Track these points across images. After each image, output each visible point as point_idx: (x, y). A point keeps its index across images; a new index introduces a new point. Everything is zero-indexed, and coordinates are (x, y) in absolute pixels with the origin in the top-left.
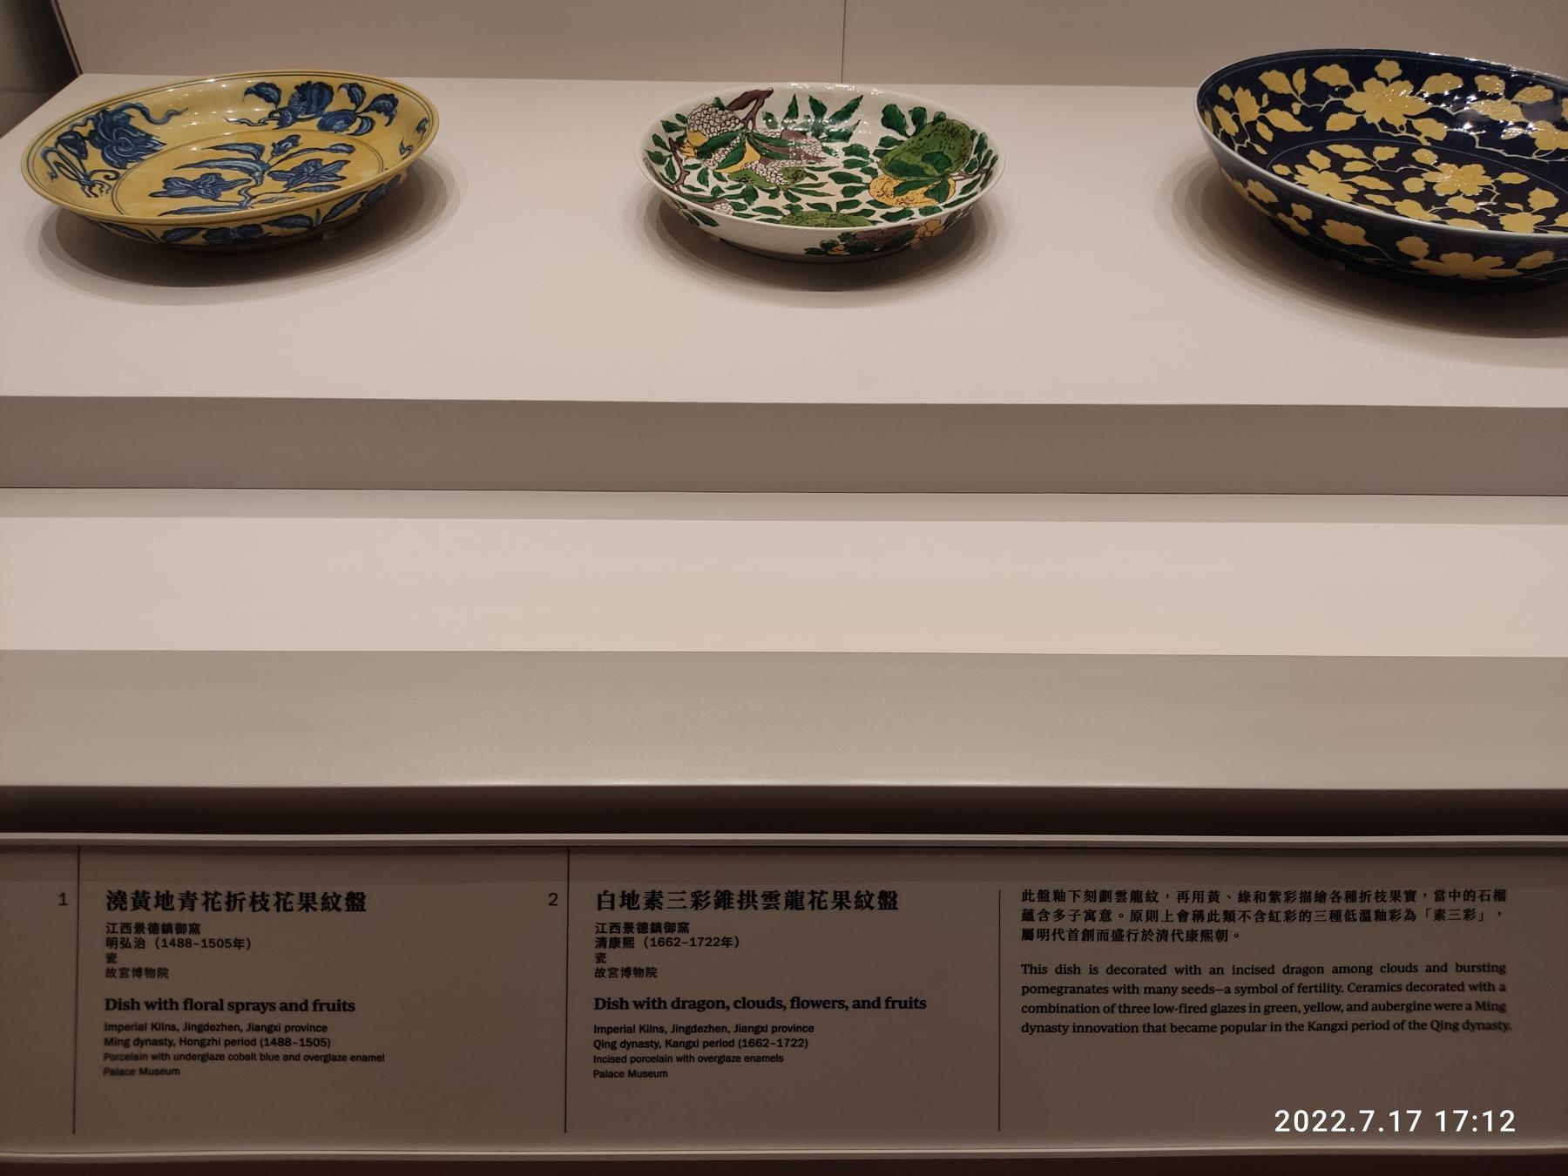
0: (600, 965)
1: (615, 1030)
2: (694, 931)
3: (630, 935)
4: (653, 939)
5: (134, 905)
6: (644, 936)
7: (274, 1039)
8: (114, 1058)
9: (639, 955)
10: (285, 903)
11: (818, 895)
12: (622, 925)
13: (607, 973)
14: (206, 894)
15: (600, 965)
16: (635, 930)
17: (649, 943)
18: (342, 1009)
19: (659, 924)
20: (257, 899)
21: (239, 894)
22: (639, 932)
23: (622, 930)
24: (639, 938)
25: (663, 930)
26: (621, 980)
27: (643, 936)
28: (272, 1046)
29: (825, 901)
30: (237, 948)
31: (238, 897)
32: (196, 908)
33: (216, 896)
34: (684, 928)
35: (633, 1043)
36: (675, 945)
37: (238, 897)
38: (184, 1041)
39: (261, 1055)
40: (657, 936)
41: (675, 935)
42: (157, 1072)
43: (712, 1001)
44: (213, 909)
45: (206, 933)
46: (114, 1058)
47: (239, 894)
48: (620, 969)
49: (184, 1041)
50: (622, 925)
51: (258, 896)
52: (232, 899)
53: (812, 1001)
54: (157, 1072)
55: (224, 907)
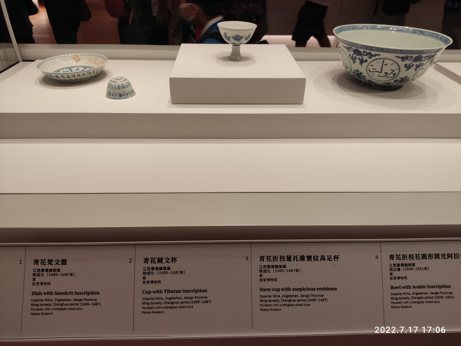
0: (391, 276)
1: (397, 294)
2: (417, 266)
3: (399, 267)
4: (405, 268)
5: (308, 259)
6: (403, 267)
7: (205, 301)
8: (145, 308)
9: (402, 273)
10: (296, 258)
11: (398, 256)
12: (397, 264)
13: (393, 278)
14: (397, 255)
15: (391, 276)
16: (400, 266)
17: (404, 269)
18: (286, 290)
19: (407, 264)
20: (281, 258)
21: (276, 256)
22: (401, 266)
23: (397, 266)
24: (401, 268)
25: (408, 266)
26: (397, 280)
27: (403, 267)
28: (194, 303)
29: (400, 257)
30: (425, 270)
31: (276, 257)
32: (394, 259)
33: (270, 257)
34: (414, 265)
35: (402, 298)
36: (420, 270)
37: (276, 257)
38: (166, 303)
39: (188, 306)
40: (406, 267)
41: (411, 267)
42: (157, 312)
43: (310, 288)
44: (399, 259)
45: (417, 266)
46: (145, 308)
47: (276, 256)
48: (397, 277)
49: (166, 303)
50: (397, 264)
51: (282, 257)
52: (275, 258)
53: (396, 287)
54: (157, 312)
55: (402, 259)
